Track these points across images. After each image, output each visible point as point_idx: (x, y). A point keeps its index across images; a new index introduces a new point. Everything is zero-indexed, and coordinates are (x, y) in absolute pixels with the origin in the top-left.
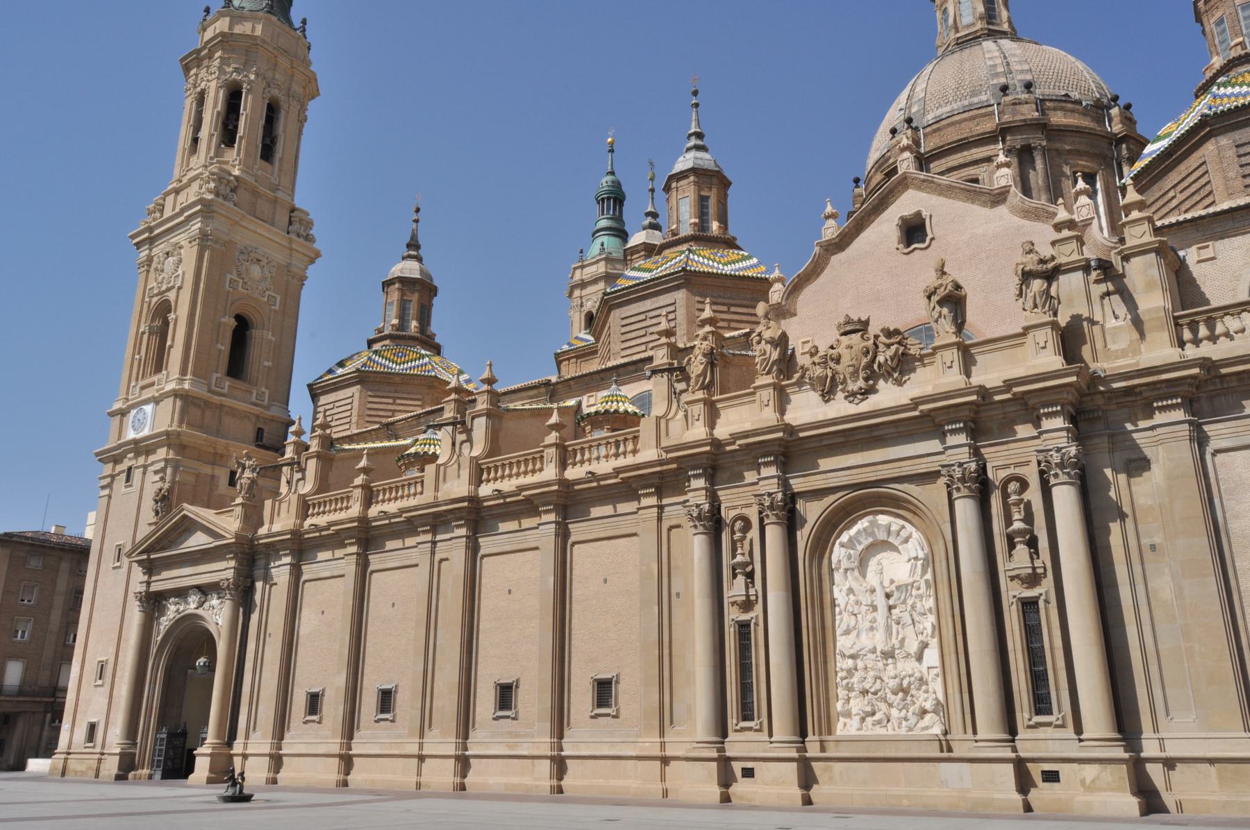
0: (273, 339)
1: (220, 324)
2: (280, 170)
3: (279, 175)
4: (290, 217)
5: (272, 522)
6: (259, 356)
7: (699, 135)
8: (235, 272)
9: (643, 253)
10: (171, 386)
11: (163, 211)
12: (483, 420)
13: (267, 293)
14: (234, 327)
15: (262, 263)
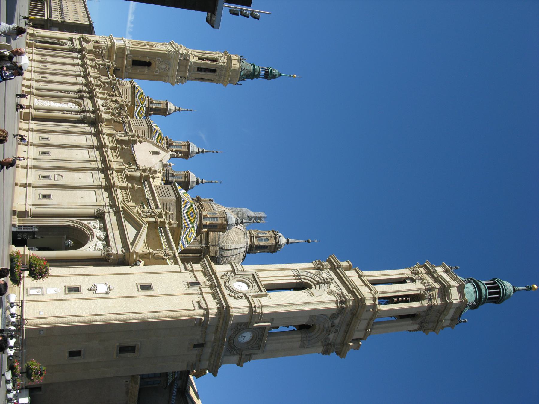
0: (146, 72)
1: (147, 57)
2: (196, 73)
3: (194, 73)
4: (183, 77)
5: (88, 55)
6: (139, 69)
7: (203, 152)
8: (161, 60)
9: (186, 174)
10: (127, 45)
11: (180, 47)
12: (110, 81)
13: (158, 70)
14: (147, 61)
15: (166, 68)
